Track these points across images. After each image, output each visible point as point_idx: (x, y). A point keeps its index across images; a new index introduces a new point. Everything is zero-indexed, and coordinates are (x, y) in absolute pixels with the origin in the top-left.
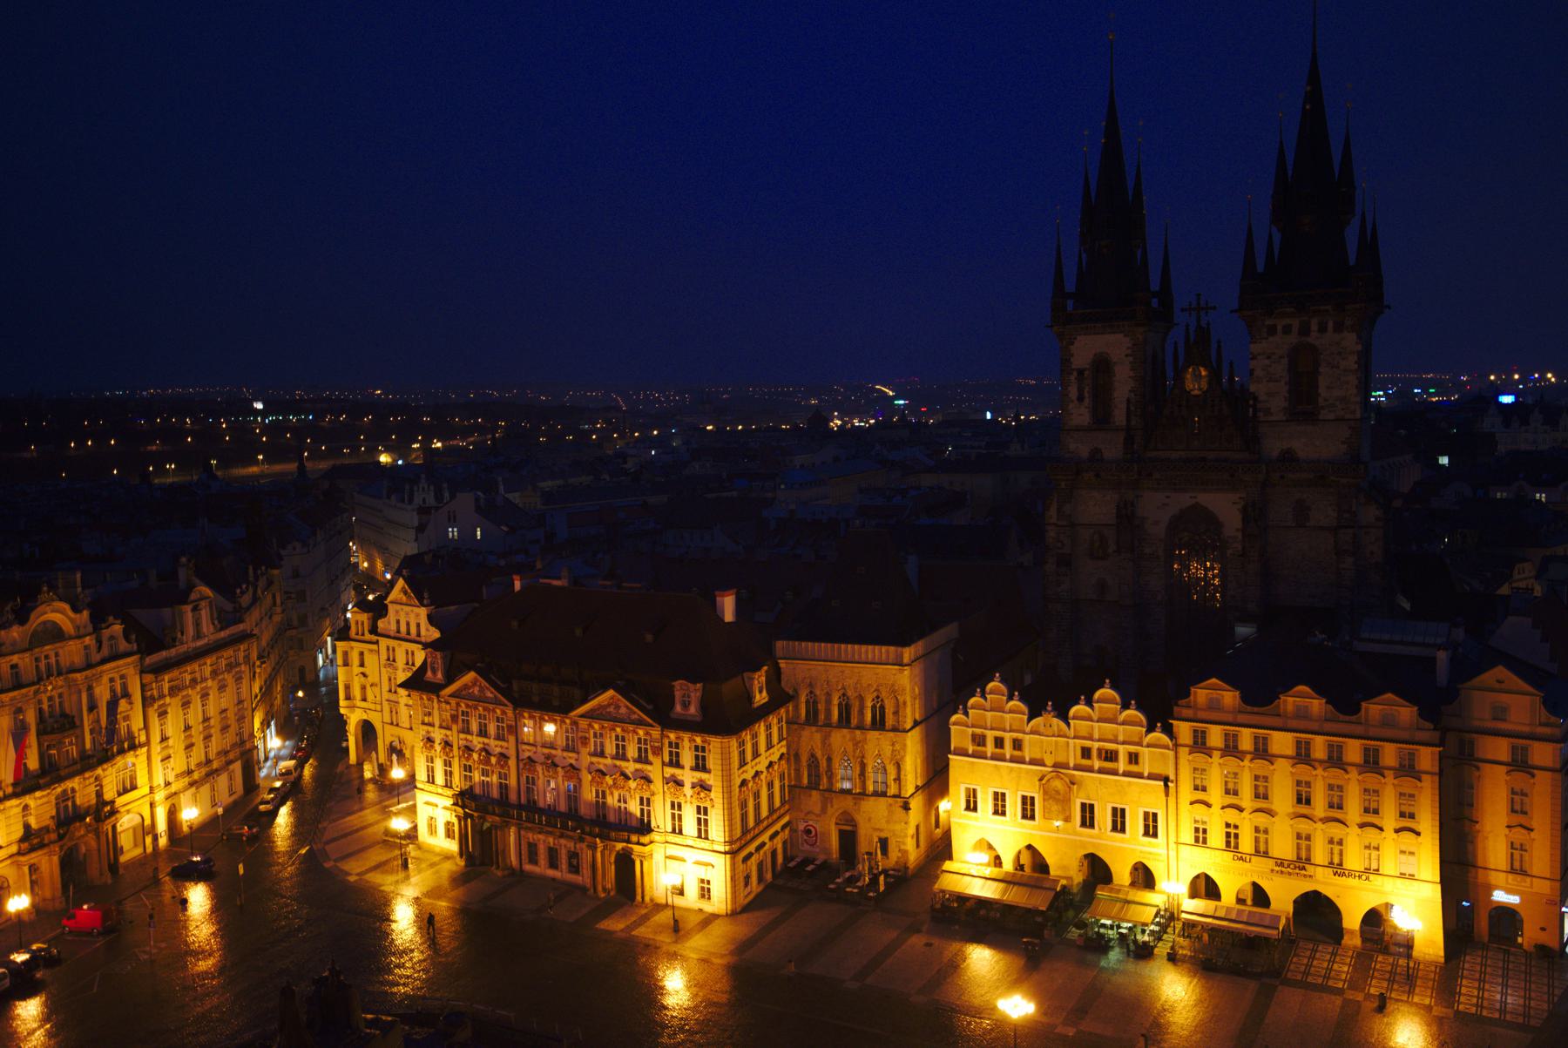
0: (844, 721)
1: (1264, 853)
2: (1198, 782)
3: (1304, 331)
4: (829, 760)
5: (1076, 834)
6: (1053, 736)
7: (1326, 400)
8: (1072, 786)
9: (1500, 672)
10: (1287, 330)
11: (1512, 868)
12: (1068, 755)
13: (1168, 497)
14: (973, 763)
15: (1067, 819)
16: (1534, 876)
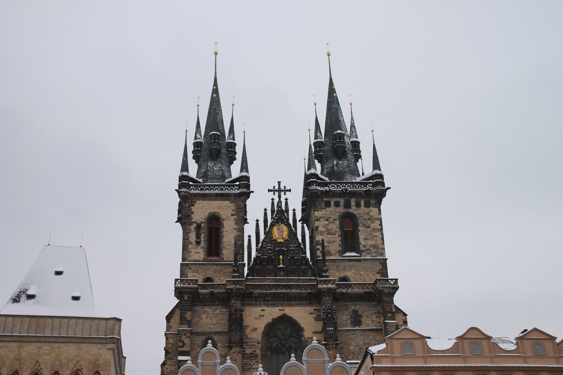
3: (348, 205)
7: (365, 247)
10: (337, 204)
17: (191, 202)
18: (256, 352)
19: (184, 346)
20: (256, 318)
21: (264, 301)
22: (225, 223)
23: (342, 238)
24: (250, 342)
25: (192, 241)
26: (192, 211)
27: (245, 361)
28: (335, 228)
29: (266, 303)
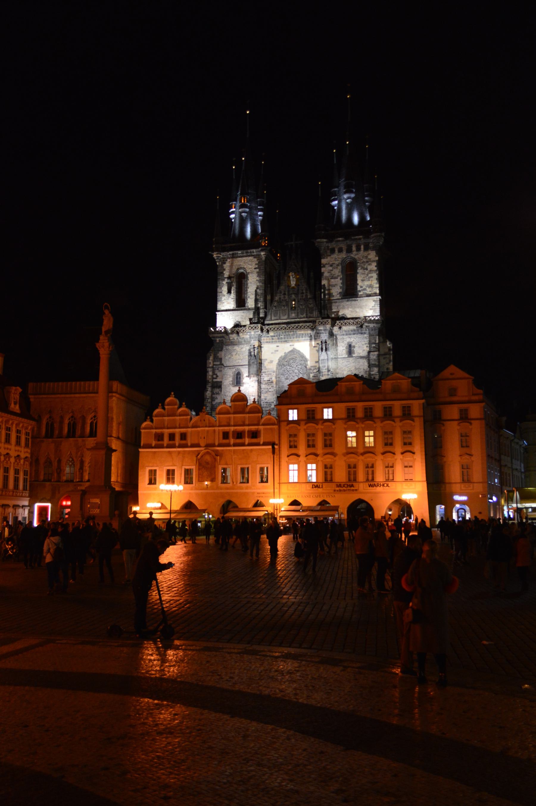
0: (72, 434)
1: (330, 481)
2: (292, 444)
4: (59, 461)
5: (218, 488)
6: (206, 427)
7: (361, 287)
8: (217, 457)
9: (452, 368)
10: (340, 251)
11: (463, 480)
12: (214, 439)
13: (278, 346)
14: (155, 452)
15: (213, 480)
16: (474, 483)
17: (223, 261)
18: (271, 379)
19: (218, 378)
20: (272, 353)
21: (278, 339)
22: (250, 276)
23: (343, 281)
24: (268, 372)
25: (224, 294)
26: (224, 268)
27: (264, 386)
28: (338, 273)
29: (280, 340)
